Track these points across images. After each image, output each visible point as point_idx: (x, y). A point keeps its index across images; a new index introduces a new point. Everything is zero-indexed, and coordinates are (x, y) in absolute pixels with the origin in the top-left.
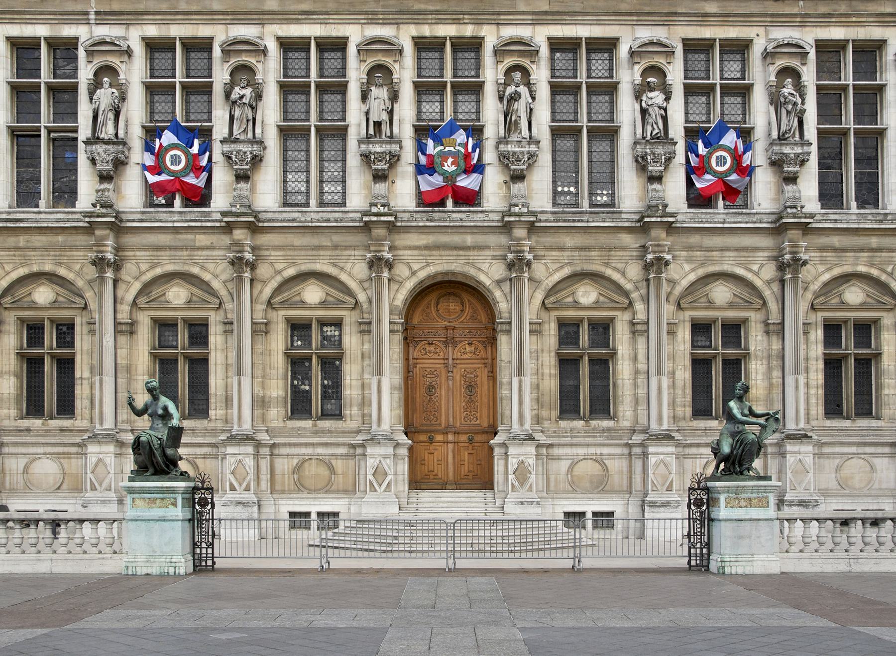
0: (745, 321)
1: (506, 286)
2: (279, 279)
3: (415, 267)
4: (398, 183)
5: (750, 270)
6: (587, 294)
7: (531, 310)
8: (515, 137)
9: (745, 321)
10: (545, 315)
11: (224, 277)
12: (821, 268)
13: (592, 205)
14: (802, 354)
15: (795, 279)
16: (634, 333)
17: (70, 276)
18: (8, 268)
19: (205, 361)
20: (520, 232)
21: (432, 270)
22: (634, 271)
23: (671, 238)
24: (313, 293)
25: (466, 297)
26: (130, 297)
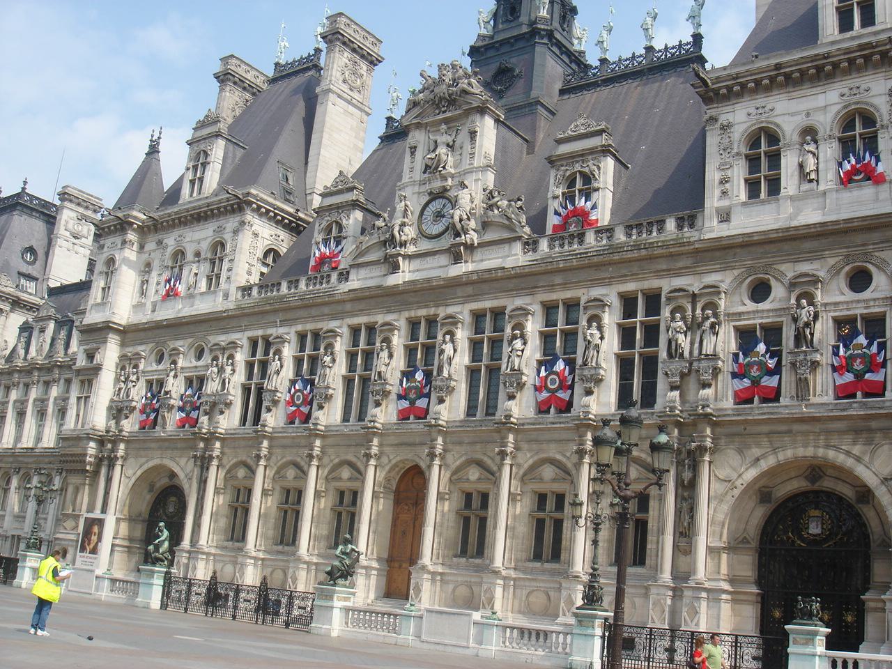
2: (331, 465)
3: (391, 457)
5: (565, 456)
21: (398, 458)
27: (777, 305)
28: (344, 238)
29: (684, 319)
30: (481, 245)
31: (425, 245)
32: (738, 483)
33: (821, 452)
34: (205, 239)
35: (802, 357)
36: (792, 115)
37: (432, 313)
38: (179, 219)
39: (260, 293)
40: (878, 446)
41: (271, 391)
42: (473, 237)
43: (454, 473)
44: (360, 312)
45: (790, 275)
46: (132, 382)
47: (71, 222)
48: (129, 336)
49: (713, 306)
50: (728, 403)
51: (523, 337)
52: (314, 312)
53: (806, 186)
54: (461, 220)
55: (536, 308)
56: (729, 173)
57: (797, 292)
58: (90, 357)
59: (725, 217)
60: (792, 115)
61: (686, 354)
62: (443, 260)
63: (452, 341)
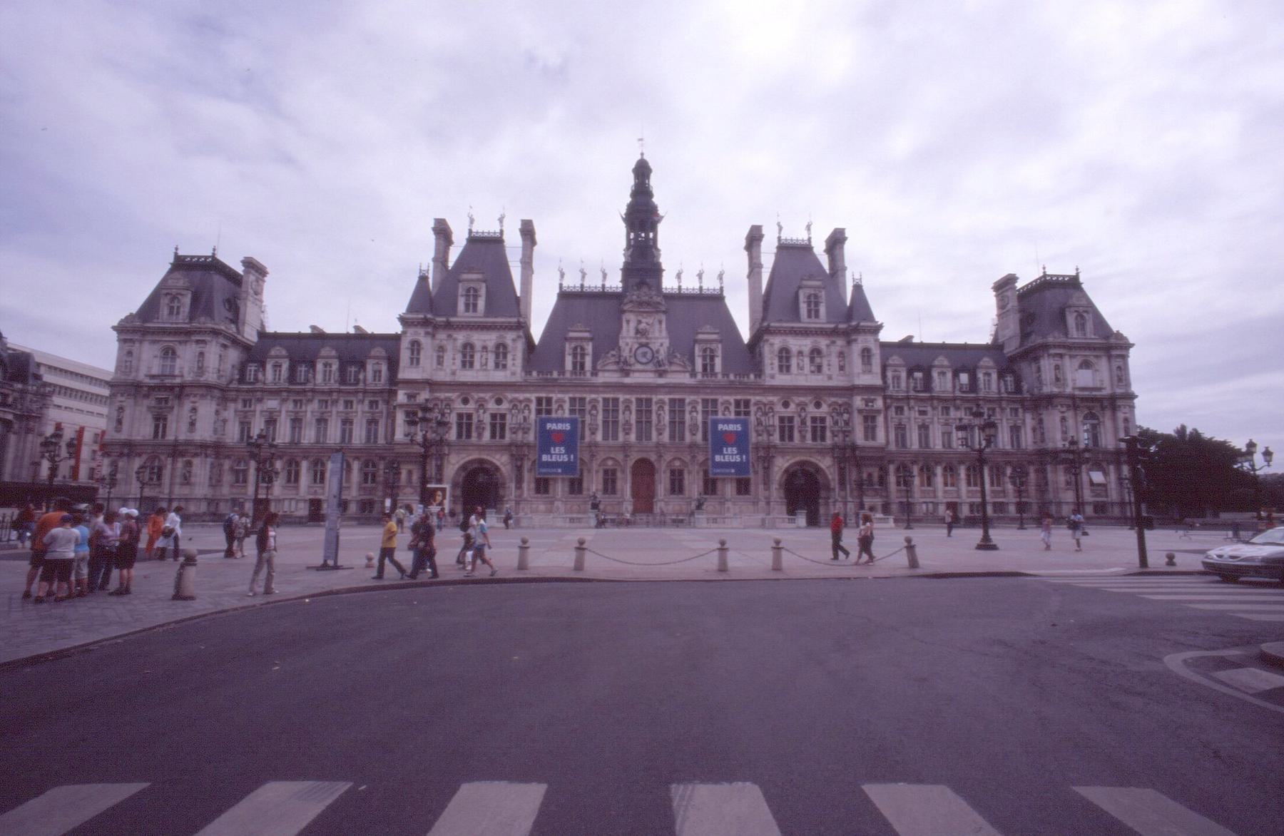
21: (640, 457)
22: (689, 457)
28: (588, 354)
29: (762, 411)
31: (639, 367)
33: (809, 459)
34: (491, 340)
39: (538, 375)
42: (667, 367)
43: (670, 462)
44: (610, 392)
45: (797, 402)
47: (254, 283)
48: (436, 387)
49: (771, 408)
51: (697, 412)
53: (800, 371)
55: (700, 401)
58: (410, 396)
59: (772, 377)
60: (795, 345)
61: (764, 424)
62: (652, 375)
63: (663, 410)
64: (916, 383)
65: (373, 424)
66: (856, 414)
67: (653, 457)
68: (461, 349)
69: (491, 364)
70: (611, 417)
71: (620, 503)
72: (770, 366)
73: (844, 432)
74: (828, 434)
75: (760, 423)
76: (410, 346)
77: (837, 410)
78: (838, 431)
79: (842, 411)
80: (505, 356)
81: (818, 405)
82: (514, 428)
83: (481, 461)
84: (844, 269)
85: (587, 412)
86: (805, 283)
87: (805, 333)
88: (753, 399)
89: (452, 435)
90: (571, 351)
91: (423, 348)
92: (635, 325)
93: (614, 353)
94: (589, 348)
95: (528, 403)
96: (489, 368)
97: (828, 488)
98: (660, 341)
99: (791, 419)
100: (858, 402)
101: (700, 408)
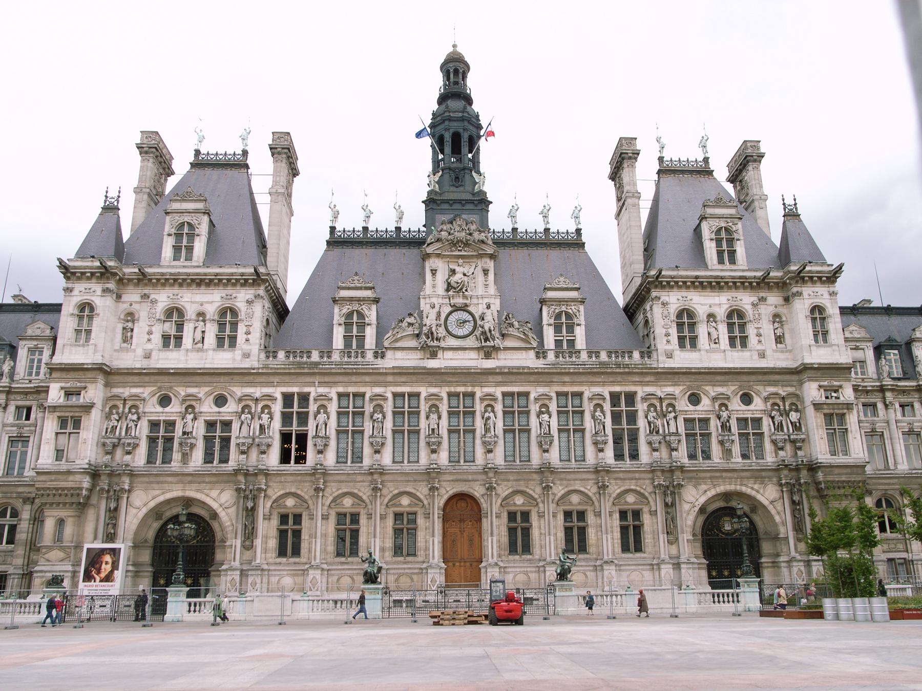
0: (586, 510)
1: (486, 497)
2: (391, 495)
3: (448, 489)
4: (441, 453)
6: (519, 500)
7: (495, 509)
8: (489, 435)
9: (586, 510)
10: (501, 509)
11: (369, 494)
12: (616, 487)
13: (520, 461)
14: (609, 526)
15: (604, 493)
16: (539, 516)
17: (303, 494)
18: (276, 491)
19: (357, 531)
20: (491, 475)
22: (538, 490)
23: (553, 476)
24: (405, 501)
25: (468, 500)
26: (328, 503)
27: (706, 408)
28: (368, 325)
29: (656, 410)
30: (506, 349)
32: (697, 503)
33: (738, 488)
35: (727, 438)
36: (702, 305)
37: (469, 390)
38: (175, 280)
39: (288, 357)
40: (766, 485)
41: (322, 437)
42: (498, 342)
44: (404, 383)
45: (713, 394)
46: (133, 421)
50: (685, 460)
52: (354, 378)
53: (713, 346)
54: (490, 331)
55: (554, 395)
56: (670, 330)
57: (719, 402)
59: (670, 356)
60: (702, 305)
61: (661, 431)
62: (473, 354)
63: (493, 411)
64: (891, 367)
65: (20, 444)
66: (810, 411)
67: (478, 491)
68: (162, 318)
69: (211, 339)
70: (406, 424)
71: (423, 572)
72: (666, 338)
73: (793, 442)
74: (768, 446)
75: (654, 431)
76: (76, 312)
77: (779, 406)
78: (785, 440)
79: (787, 408)
80: (234, 325)
81: (747, 399)
82: (244, 444)
83: (188, 502)
84: (764, 198)
85: (367, 414)
86: (710, 211)
87: (717, 285)
88: (641, 391)
89: (140, 458)
90: (342, 320)
91: (98, 315)
92: (447, 277)
93: (411, 320)
94: (371, 314)
95: (269, 403)
96: (205, 347)
97: (775, 538)
98: (486, 301)
99: (705, 421)
100: (812, 391)
101: (553, 407)
